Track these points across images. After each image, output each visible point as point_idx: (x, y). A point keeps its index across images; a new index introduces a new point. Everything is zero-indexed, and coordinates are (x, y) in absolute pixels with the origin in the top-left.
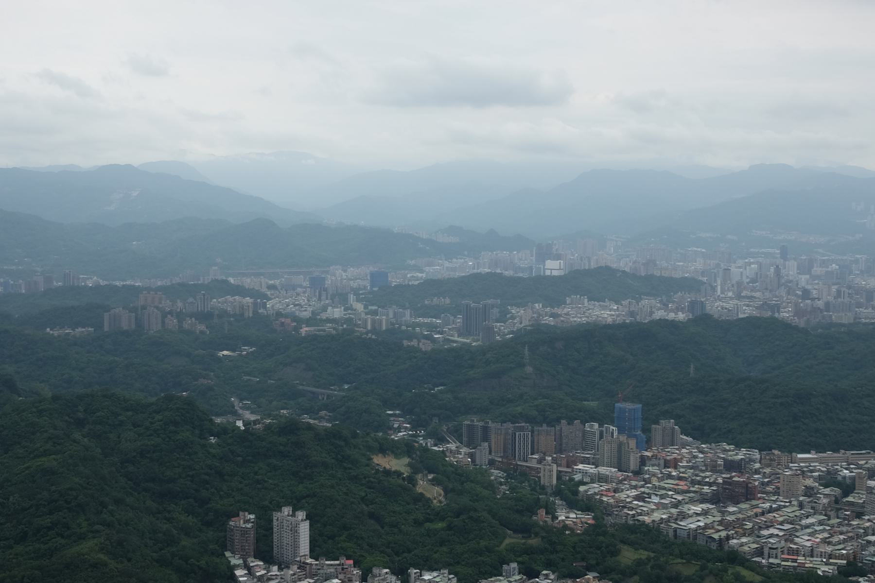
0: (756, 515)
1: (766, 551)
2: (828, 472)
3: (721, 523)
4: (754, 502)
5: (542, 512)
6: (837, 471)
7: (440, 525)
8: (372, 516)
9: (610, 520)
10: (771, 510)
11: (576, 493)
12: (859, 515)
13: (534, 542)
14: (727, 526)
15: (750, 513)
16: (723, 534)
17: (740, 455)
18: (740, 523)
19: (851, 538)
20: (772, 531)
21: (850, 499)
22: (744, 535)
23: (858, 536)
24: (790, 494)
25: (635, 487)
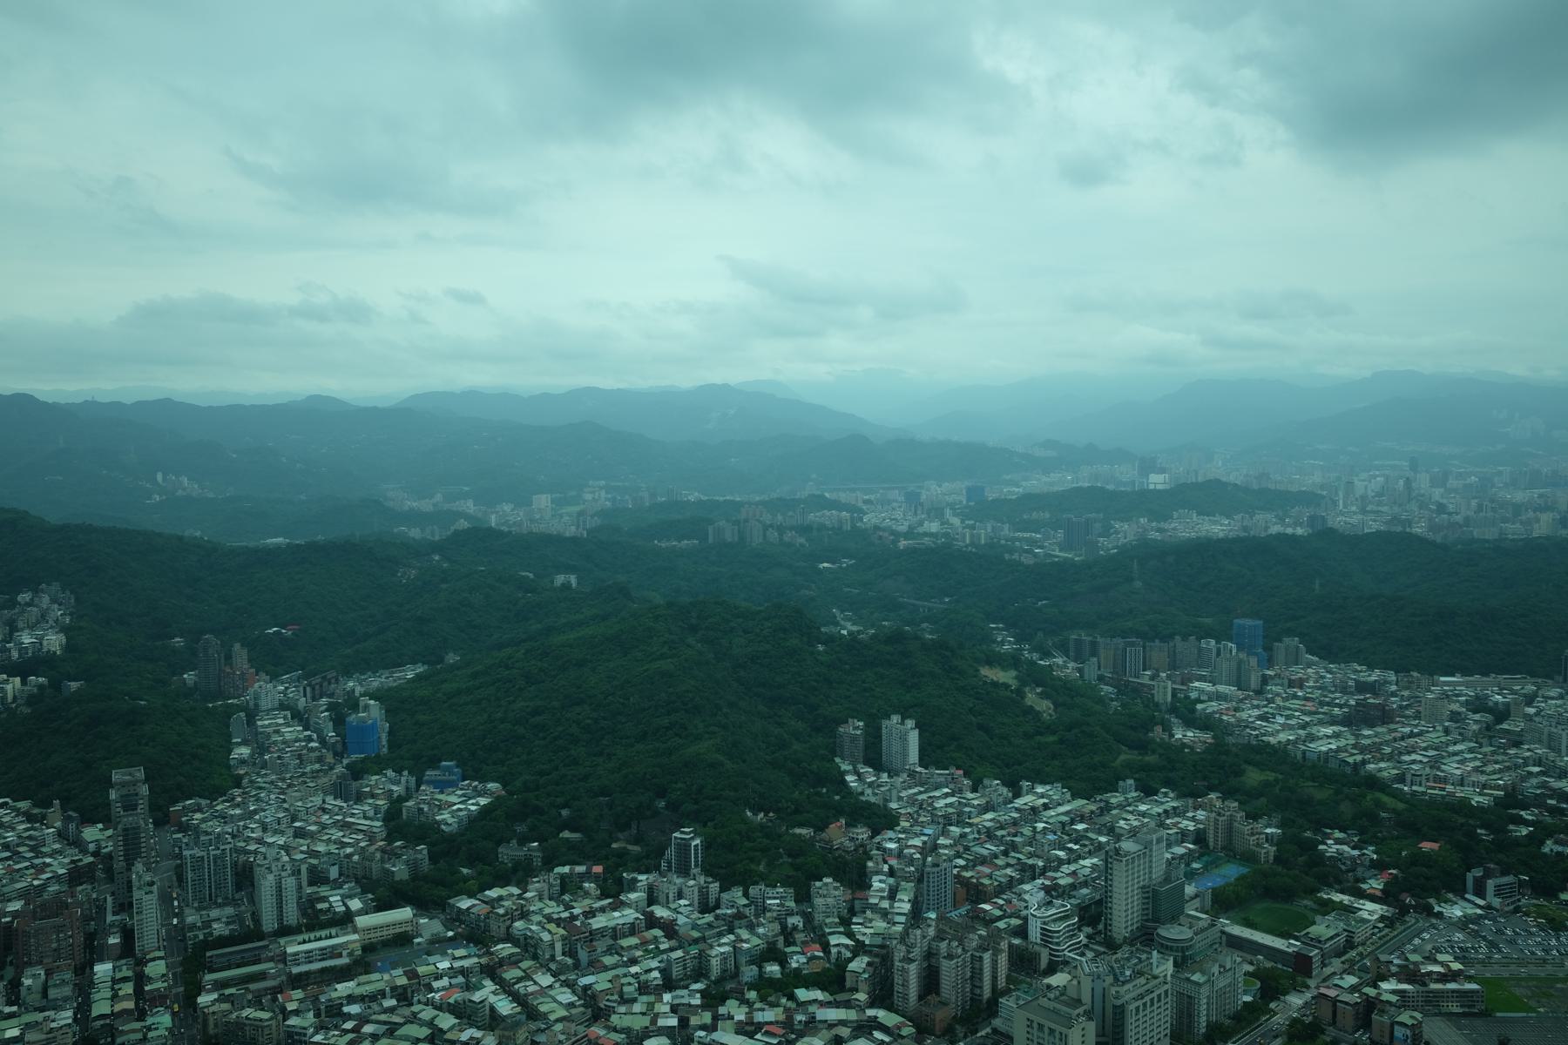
0: (1395, 740)
1: (1408, 777)
2: (1477, 697)
3: (1355, 746)
4: (1392, 726)
5: (1159, 729)
6: (1487, 696)
7: (1051, 739)
8: (980, 727)
9: (1231, 740)
10: (1412, 735)
11: (1194, 710)
12: (1517, 744)
13: (1151, 759)
14: (1363, 750)
15: (1388, 737)
16: (1359, 758)
17: (1375, 676)
18: (1376, 748)
19: (1508, 768)
20: (1414, 757)
21: (1505, 726)
22: (1382, 760)
23: (1517, 766)
24: (1434, 719)
25: (1257, 707)
